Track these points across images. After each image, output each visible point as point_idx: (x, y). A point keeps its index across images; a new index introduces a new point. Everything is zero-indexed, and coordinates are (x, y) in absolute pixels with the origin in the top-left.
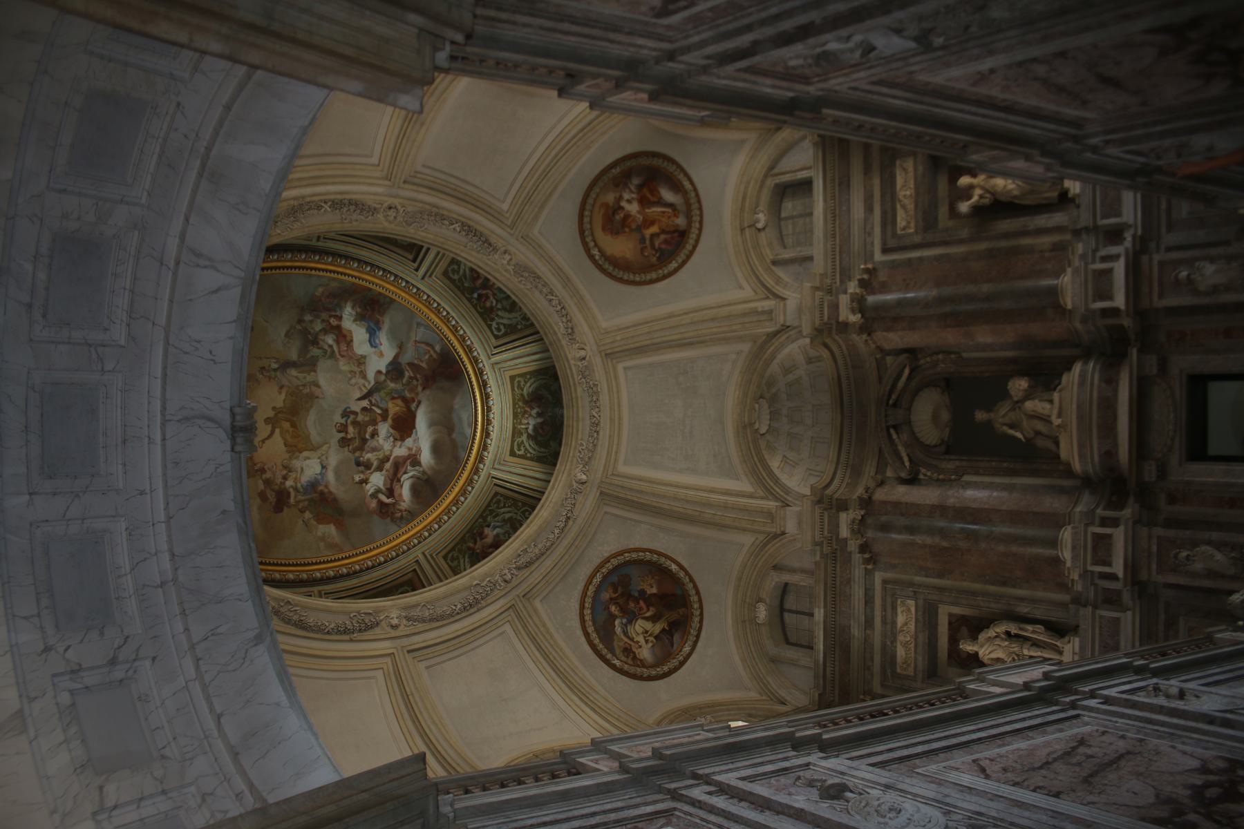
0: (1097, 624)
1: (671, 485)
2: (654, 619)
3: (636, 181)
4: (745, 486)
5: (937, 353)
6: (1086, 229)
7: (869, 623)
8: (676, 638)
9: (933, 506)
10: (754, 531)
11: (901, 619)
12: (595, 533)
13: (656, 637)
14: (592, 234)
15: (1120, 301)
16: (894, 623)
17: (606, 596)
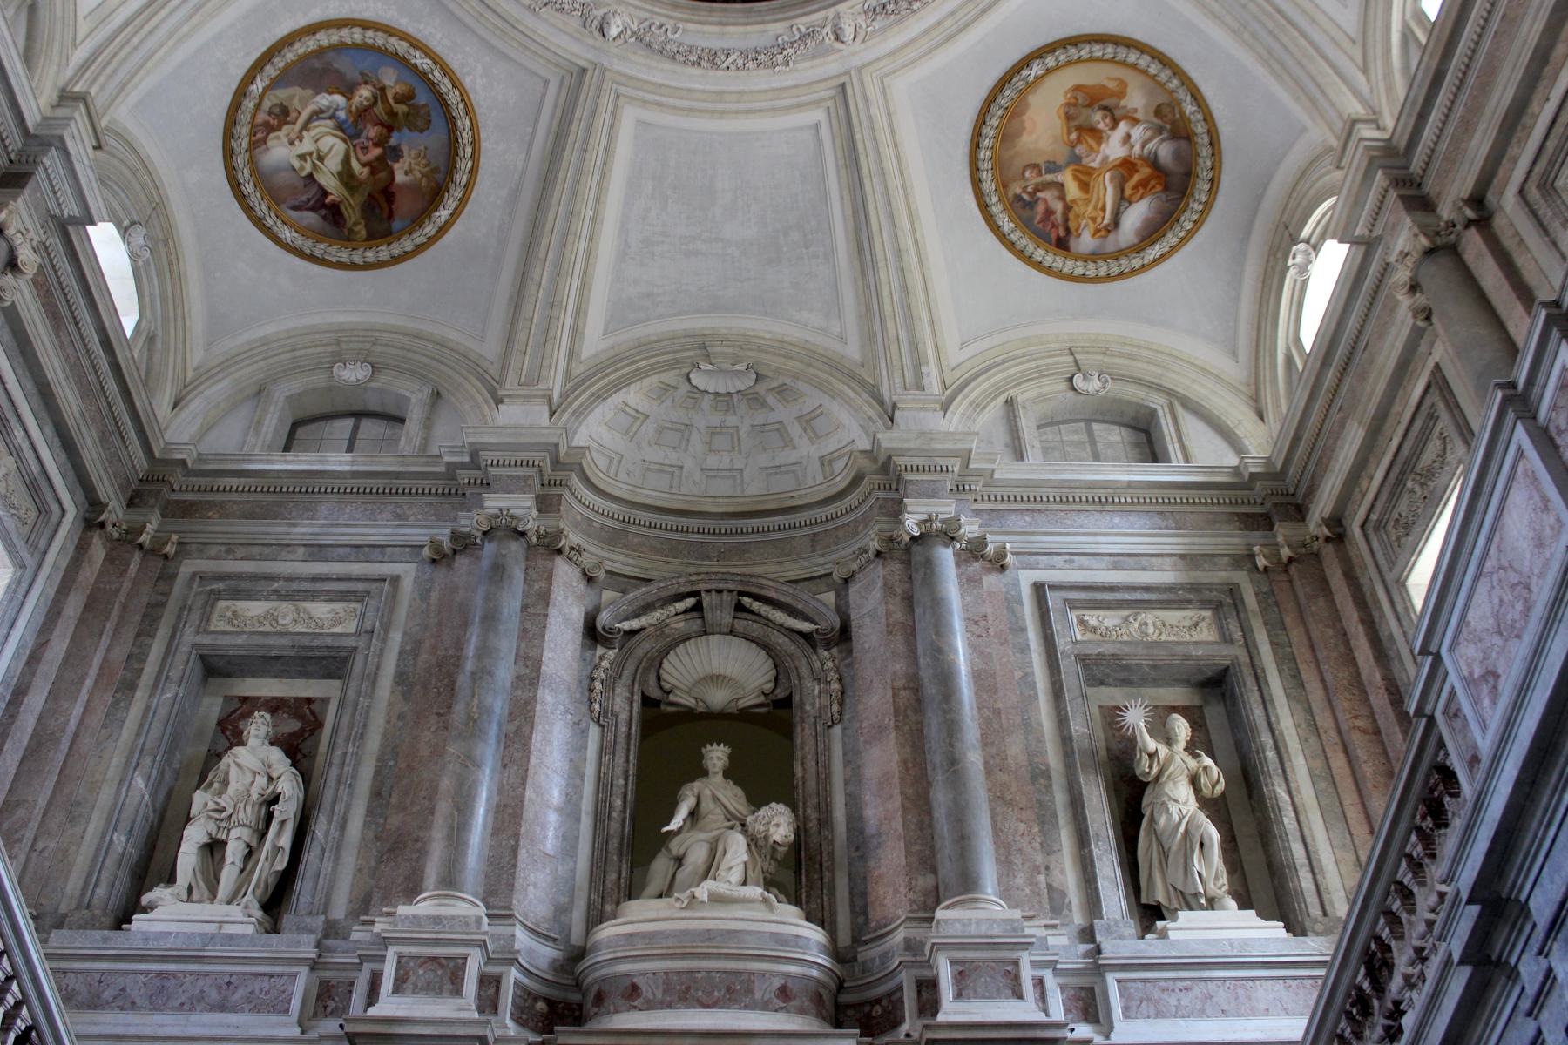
0: (278, 969)
1: (596, 210)
2: (346, 176)
3: (1165, 151)
4: (594, 342)
5: (840, 680)
6: (1099, 951)
7: (318, 551)
8: (311, 218)
9: (540, 662)
10: (505, 358)
11: (320, 610)
12: (505, 57)
13: (310, 177)
14: (1069, 63)
15: (952, 1011)
16: (313, 596)
17: (390, 78)
